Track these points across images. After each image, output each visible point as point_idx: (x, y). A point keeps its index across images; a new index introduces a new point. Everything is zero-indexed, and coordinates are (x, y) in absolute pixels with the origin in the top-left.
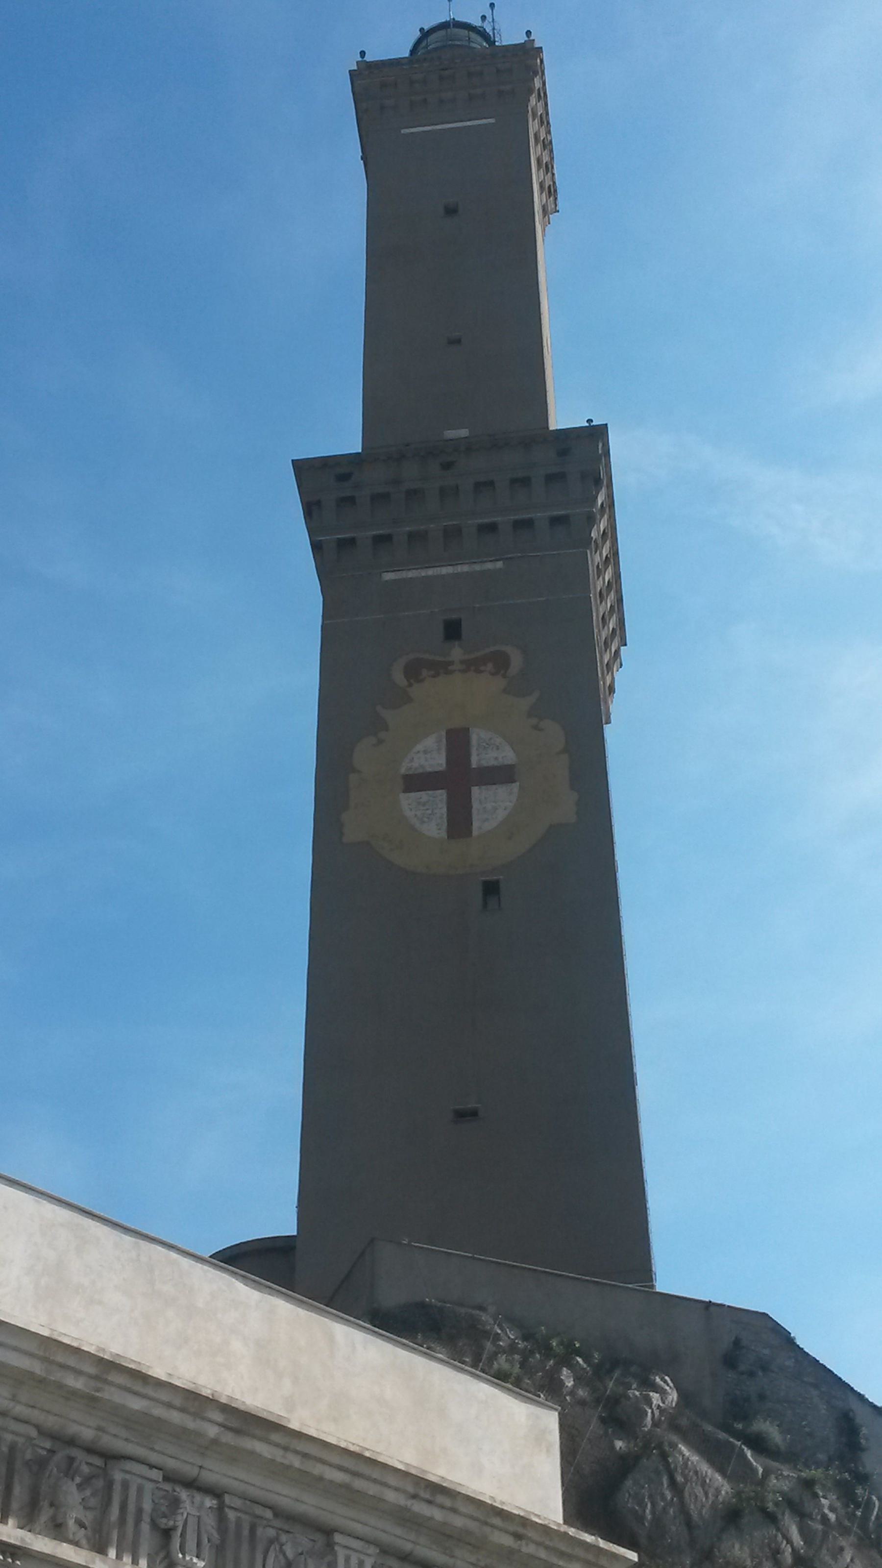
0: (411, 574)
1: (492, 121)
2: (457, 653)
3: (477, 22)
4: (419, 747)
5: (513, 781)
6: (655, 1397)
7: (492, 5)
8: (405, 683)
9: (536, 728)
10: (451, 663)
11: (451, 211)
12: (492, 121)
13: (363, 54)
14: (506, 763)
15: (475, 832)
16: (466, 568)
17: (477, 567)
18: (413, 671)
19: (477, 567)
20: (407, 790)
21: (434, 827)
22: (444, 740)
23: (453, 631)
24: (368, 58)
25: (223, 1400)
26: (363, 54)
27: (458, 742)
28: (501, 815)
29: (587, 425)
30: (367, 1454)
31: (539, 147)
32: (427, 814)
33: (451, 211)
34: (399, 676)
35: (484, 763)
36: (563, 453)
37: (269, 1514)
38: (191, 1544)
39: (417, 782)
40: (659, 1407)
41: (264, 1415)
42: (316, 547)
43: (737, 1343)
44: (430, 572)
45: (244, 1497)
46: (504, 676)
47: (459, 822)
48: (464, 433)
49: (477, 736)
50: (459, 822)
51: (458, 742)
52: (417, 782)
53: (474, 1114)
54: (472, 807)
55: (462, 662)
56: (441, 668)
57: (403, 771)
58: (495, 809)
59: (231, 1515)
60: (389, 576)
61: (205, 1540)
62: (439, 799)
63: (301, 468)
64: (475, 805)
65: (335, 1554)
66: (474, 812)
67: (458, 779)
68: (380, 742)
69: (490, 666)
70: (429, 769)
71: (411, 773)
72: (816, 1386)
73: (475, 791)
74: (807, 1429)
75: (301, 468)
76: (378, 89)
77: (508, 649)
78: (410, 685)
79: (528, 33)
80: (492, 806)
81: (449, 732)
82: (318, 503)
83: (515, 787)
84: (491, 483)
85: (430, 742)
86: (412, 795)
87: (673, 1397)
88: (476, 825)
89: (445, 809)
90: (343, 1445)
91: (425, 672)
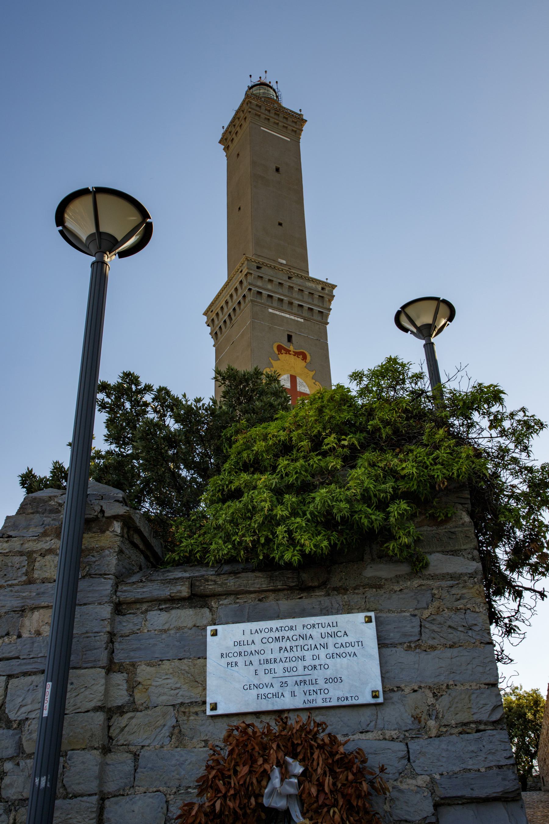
0: (277, 313)
1: (289, 140)
7: (277, 82)
9: (314, 383)
10: (290, 351)
12: (289, 140)
16: (293, 317)
17: (296, 319)
19: (296, 319)
23: (290, 338)
33: (277, 170)
34: (275, 349)
44: (283, 314)
46: (305, 362)
48: (284, 262)
49: (299, 380)
55: (293, 352)
56: (288, 352)
60: (270, 310)
77: (306, 352)
79: (300, 110)
91: (283, 351)
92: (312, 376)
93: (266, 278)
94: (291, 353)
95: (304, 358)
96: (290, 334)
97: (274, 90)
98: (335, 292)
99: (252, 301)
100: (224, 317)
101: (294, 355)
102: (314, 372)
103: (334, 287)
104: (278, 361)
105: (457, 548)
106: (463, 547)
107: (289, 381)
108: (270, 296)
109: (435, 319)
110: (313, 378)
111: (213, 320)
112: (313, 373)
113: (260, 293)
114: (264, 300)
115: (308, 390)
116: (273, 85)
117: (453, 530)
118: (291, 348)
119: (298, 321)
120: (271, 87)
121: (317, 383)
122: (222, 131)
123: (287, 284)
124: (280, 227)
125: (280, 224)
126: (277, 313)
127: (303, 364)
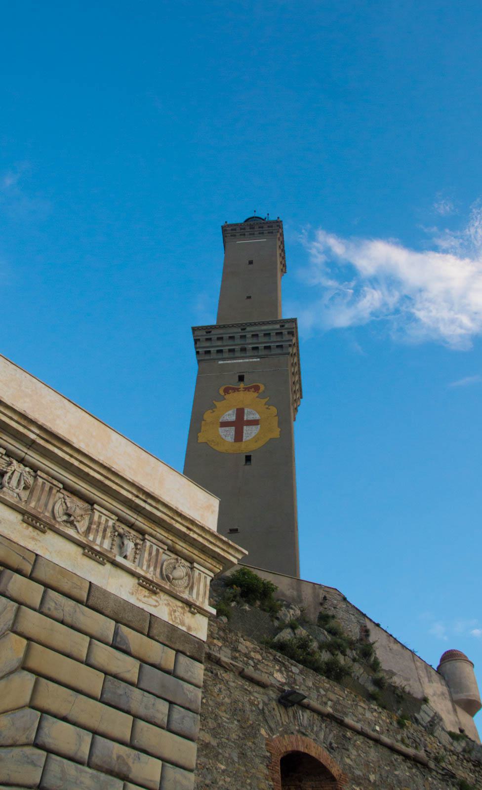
0: (228, 362)
2: (242, 385)
3: (263, 218)
4: (227, 413)
5: (258, 424)
6: (292, 612)
7: (268, 214)
8: (224, 394)
9: (267, 408)
10: (240, 388)
11: (251, 262)
13: (226, 222)
14: (256, 419)
15: (244, 441)
16: (247, 360)
18: (227, 391)
19: (251, 360)
20: (221, 427)
22: (235, 412)
23: (241, 378)
24: (228, 223)
25: (40, 423)
26: (226, 222)
27: (240, 412)
28: (253, 435)
30: (113, 469)
31: (282, 266)
32: (228, 435)
34: (221, 392)
35: (249, 419)
37: (61, 486)
38: (14, 482)
39: (225, 424)
40: (293, 614)
41: (61, 437)
42: (198, 353)
43: (325, 598)
45: (47, 473)
46: (258, 392)
47: (239, 437)
50: (239, 437)
51: (240, 412)
52: (225, 424)
54: (242, 432)
55: (243, 388)
57: (220, 421)
58: (251, 433)
59: (40, 480)
61: (22, 482)
62: (233, 428)
63: (194, 329)
64: (245, 432)
65: (94, 512)
66: (244, 434)
67: (239, 424)
68: (214, 411)
69: (253, 389)
70: (229, 420)
71: (224, 421)
72: (353, 615)
73: (245, 427)
74: (349, 629)
75: (194, 329)
76: (230, 232)
77: (258, 384)
78: (225, 395)
79: (278, 218)
80: (250, 432)
81: (238, 410)
83: (259, 426)
84: (257, 335)
85: (230, 412)
86: (222, 428)
87: (298, 612)
88: (244, 438)
89: (234, 433)
90: (101, 462)
91: (230, 391)
92: (265, 402)
93: (214, 337)
94: (242, 389)
95: (257, 388)
96: (240, 374)
101: (245, 390)
102: (268, 398)
104: (225, 401)
107: (235, 415)
110: (265, 404)
114: (214, 355)
115: (258, 416)
119: (251, 362)
124: (249, 300)
125: (249, 297)
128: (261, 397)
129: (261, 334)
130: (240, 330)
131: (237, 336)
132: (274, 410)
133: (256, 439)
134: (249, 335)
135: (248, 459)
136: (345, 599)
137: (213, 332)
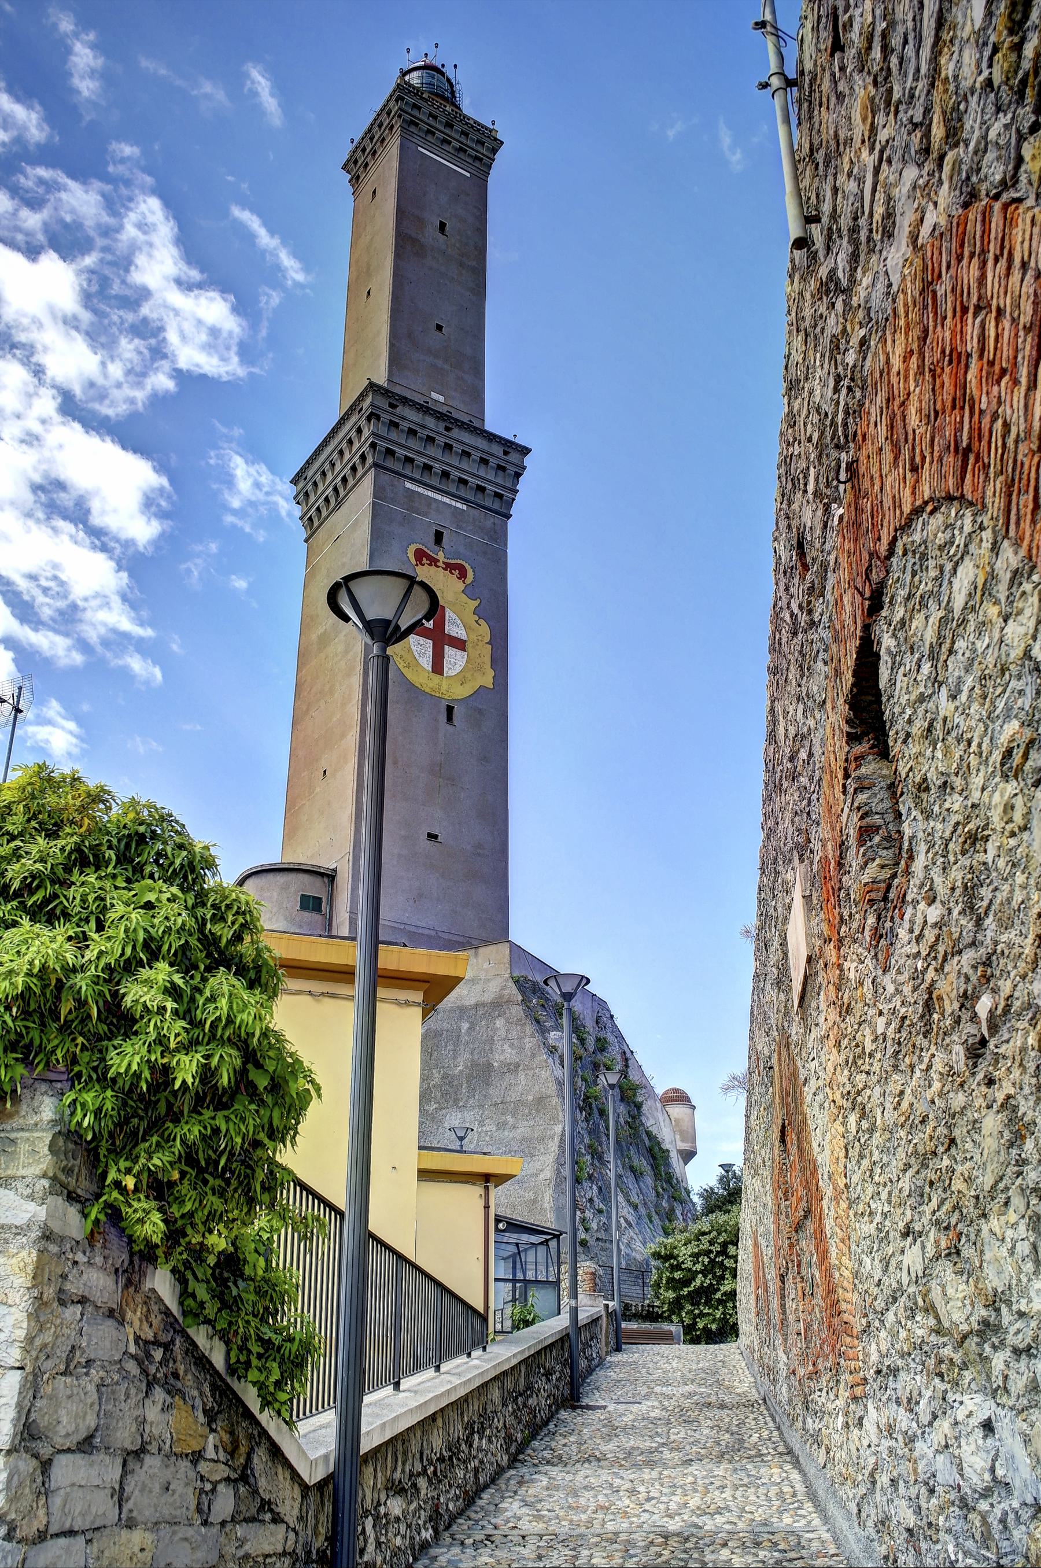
0: (420, 490)
16: (447, 501)
17: (454, 503)
19: (454, 503)
21: (426, 662)
23: (439, 537)
28: (458, 669)
29: (512, 439)
33: (442, 226)
36: (506, 453)
44: (430, 494)
47: (438, 667)
48: (441, 399)
53: (436, 837)
56: (433, 562)
60: (408, 485)
80: (454, 660)
82: (378, 418)
84: (468, 455)
91: (425, 561)
93: (405, 425)
94: (440, 564)
95: (463, 575)
97: (449, 80)
98: (527, 461)
99: (375, 465)
100: (325, 489)
103: (525, 451)
105: (9, 1172)
106: (21, 1172)
108: (409, 460)
109: (400, 611)
111: (307, 494)
112: (476, 603)
113: (390, 452)
114: (398, 467)
116: (449, 72)
117: (13, 1135)
118: (441, 556)
120: (443, 74)
121: (481, 621)
122: (350, 147)
123: (441, 440)
126: (420, 490)
127: (461, 586)
128: (470, 591)
129: (476, 455)
130: (442, 430)
131: (441, 440)
132: (484, 630)
133: (462, 678)
134: (458, 448)
135: (450, 710)
136: (612, 1017)
137: (399, 410)
